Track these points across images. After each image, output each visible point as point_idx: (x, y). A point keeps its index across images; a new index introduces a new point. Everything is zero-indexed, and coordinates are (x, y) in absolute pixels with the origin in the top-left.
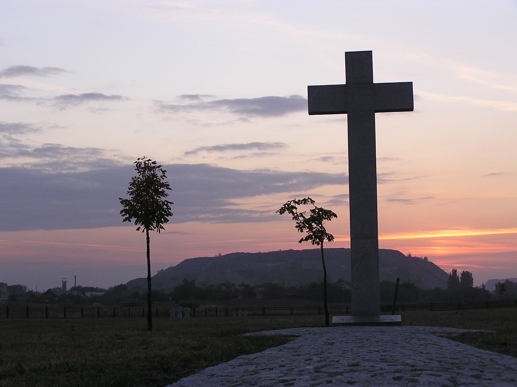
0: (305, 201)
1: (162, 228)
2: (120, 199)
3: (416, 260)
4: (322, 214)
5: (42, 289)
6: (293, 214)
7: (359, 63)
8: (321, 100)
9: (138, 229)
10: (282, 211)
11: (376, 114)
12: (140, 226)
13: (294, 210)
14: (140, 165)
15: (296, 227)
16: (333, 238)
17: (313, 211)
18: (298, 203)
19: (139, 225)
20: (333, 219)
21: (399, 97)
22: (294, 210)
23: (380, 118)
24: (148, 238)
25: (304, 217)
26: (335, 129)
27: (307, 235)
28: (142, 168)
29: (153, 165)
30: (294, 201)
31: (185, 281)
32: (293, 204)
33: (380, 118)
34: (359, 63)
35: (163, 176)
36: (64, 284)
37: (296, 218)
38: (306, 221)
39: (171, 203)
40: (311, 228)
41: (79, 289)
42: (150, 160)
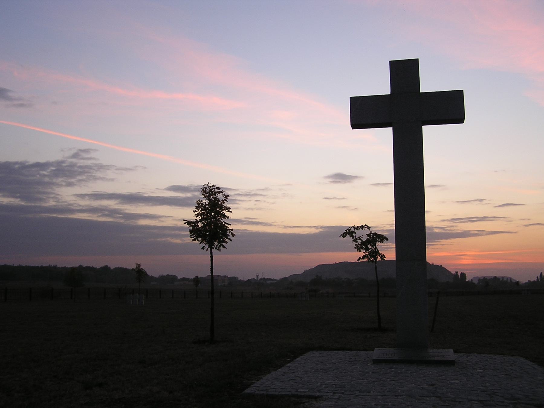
0: (362, 227)
1: (224, 247)
2: (185, 220)
3: (437, 266)
4: (376, 238)
5: (246, 279)
6: (353, 237)
7: (404, 72)
8: (364, 113)
9: (203, 248)
10: (344, 235)
11: (424, 127)
12: (204, 245)
13: (354, 234)
14: (206, 190)
15: (355, 248)
16: (385, 257)
17: (369, 235)
18: (357, 228)
19: (203, 245)
20: (385, 241)
21: (449, 108)
22: (354, 234)
23: (428, 131)
24: (212, 257)
25: (361, 240)
26: (381, 141)
27: (364, 254)
28: (207, 193)
29: (217, 190)
30: (354, 227)
31: (317, 276)
32: (353, 229)
33: (428, 131)
34: (404, 72)
35: (225, 200)
36: (257, 277)
37: (355, 240)
38: (363, 243)
39: (229, 225)
40: (367, 249)
41: (264, 279)
42: (213, 186)
